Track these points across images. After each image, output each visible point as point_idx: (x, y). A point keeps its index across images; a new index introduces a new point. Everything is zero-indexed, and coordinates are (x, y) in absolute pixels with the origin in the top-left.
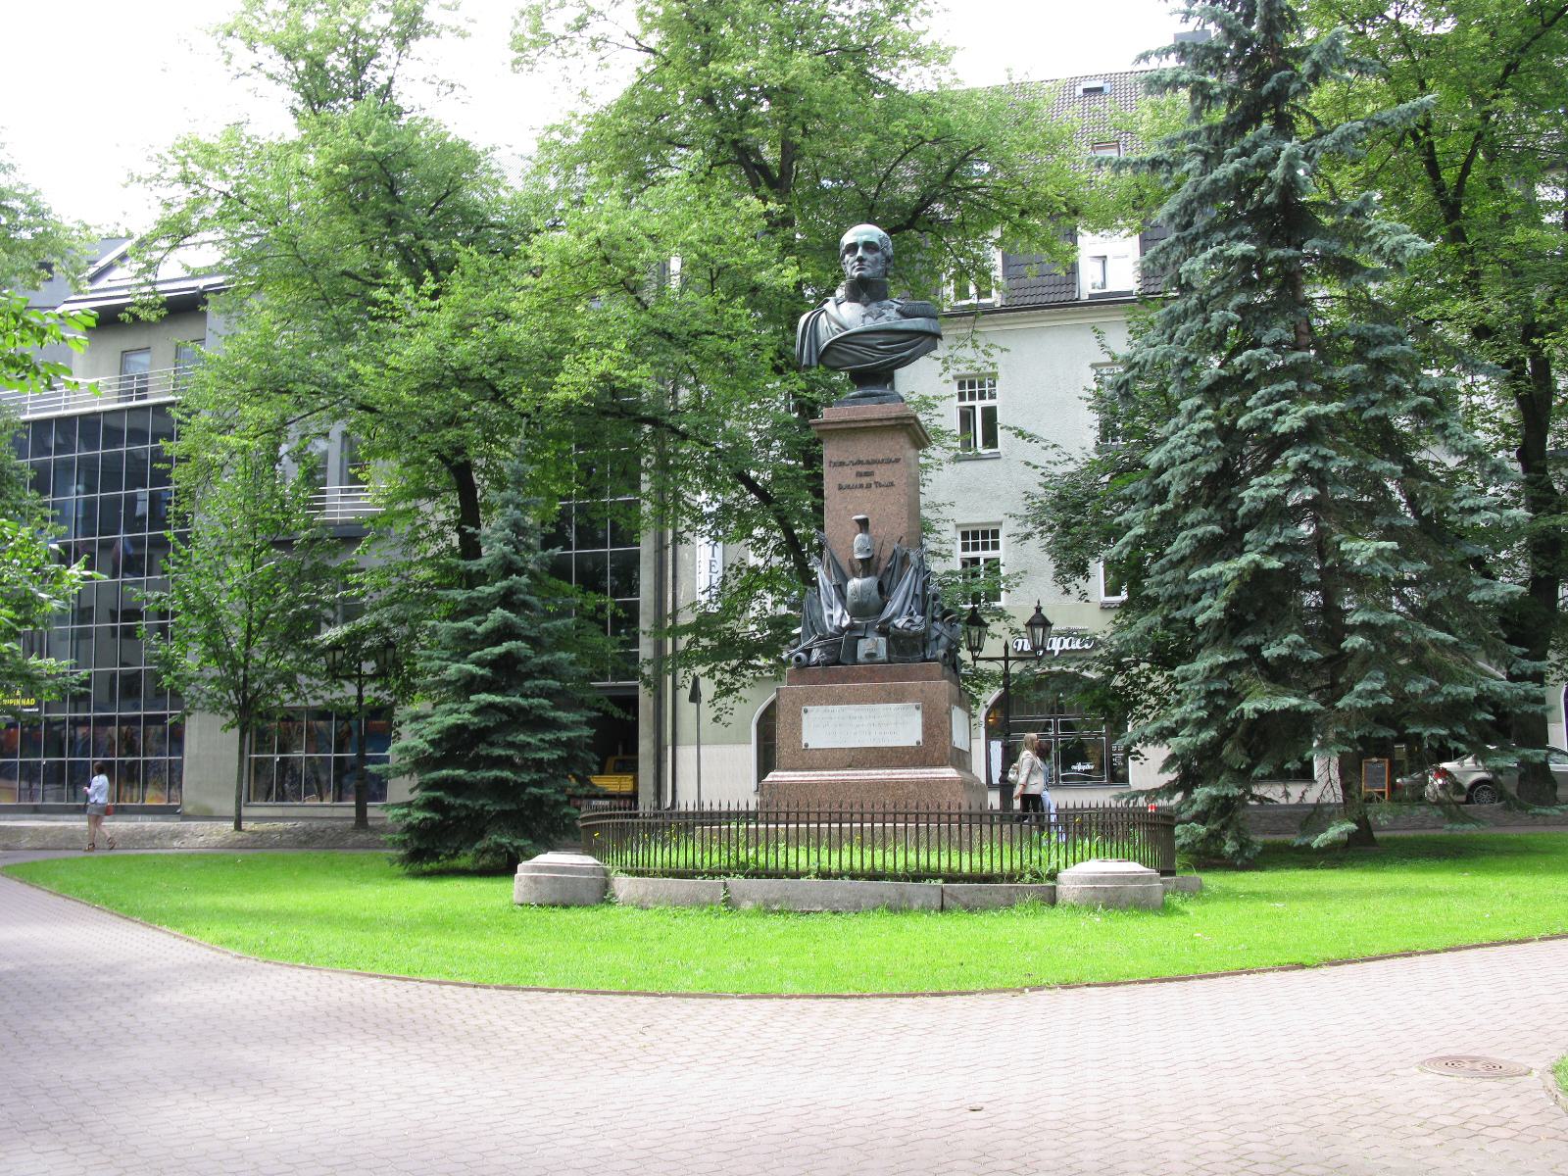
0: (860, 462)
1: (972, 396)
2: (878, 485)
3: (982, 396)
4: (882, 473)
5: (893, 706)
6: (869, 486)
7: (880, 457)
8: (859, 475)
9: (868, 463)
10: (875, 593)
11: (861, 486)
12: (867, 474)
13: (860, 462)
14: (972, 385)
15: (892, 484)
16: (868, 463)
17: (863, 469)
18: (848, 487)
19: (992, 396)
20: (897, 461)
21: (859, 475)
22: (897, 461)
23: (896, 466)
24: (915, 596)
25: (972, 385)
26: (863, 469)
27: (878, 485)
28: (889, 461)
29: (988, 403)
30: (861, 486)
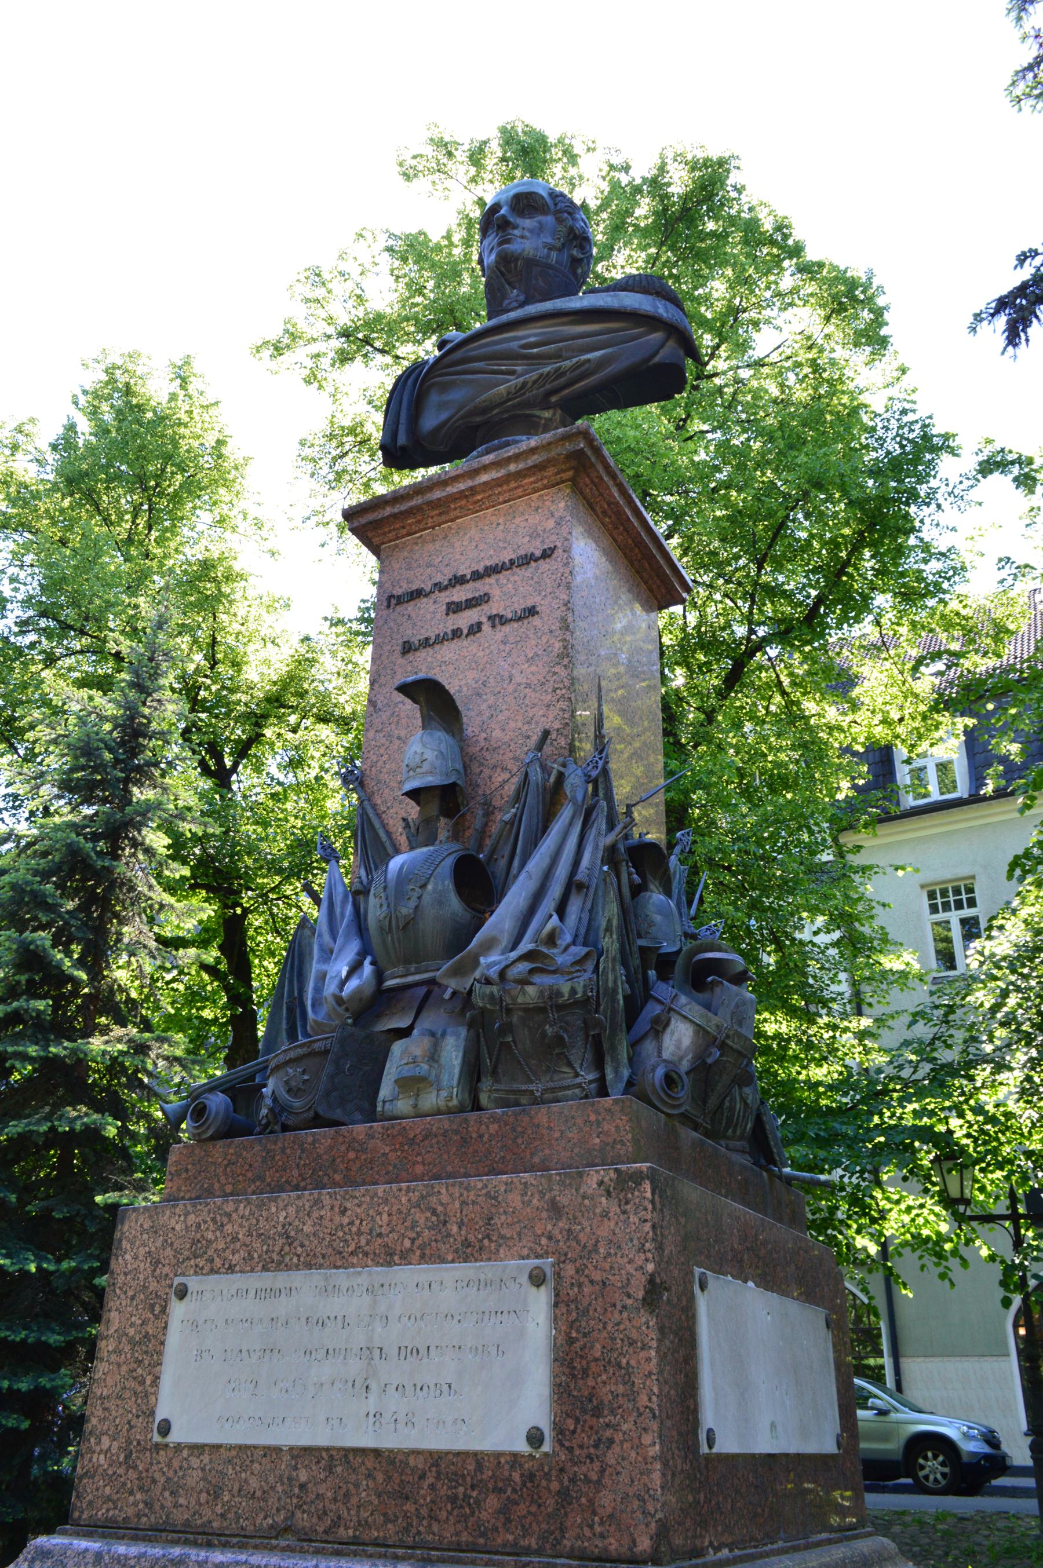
0: (459, 580)
1: (946, 907)
3: (959, 905)
4: (506, 593)
5: (452, 1274)
6: (475, 629)
7: (507, 556)
8: (454, 608)
9: (477, 576)
10: (442, 883)
11: (457, 634)
13: (459, 580)
14: (944, 893)
15: (532, 612)
16: (477, 576)
17: (459, 594)
18: (426, 643)
19: (972, 903)
20: (547, 554)
21: (454, 608)
22: (547, 554)
23: (544, 565)
24: (573, 886)
25: (944, 893)
26: (459, 594)
28: (528, 560)
29: (967, 912)
30: (457, 634)
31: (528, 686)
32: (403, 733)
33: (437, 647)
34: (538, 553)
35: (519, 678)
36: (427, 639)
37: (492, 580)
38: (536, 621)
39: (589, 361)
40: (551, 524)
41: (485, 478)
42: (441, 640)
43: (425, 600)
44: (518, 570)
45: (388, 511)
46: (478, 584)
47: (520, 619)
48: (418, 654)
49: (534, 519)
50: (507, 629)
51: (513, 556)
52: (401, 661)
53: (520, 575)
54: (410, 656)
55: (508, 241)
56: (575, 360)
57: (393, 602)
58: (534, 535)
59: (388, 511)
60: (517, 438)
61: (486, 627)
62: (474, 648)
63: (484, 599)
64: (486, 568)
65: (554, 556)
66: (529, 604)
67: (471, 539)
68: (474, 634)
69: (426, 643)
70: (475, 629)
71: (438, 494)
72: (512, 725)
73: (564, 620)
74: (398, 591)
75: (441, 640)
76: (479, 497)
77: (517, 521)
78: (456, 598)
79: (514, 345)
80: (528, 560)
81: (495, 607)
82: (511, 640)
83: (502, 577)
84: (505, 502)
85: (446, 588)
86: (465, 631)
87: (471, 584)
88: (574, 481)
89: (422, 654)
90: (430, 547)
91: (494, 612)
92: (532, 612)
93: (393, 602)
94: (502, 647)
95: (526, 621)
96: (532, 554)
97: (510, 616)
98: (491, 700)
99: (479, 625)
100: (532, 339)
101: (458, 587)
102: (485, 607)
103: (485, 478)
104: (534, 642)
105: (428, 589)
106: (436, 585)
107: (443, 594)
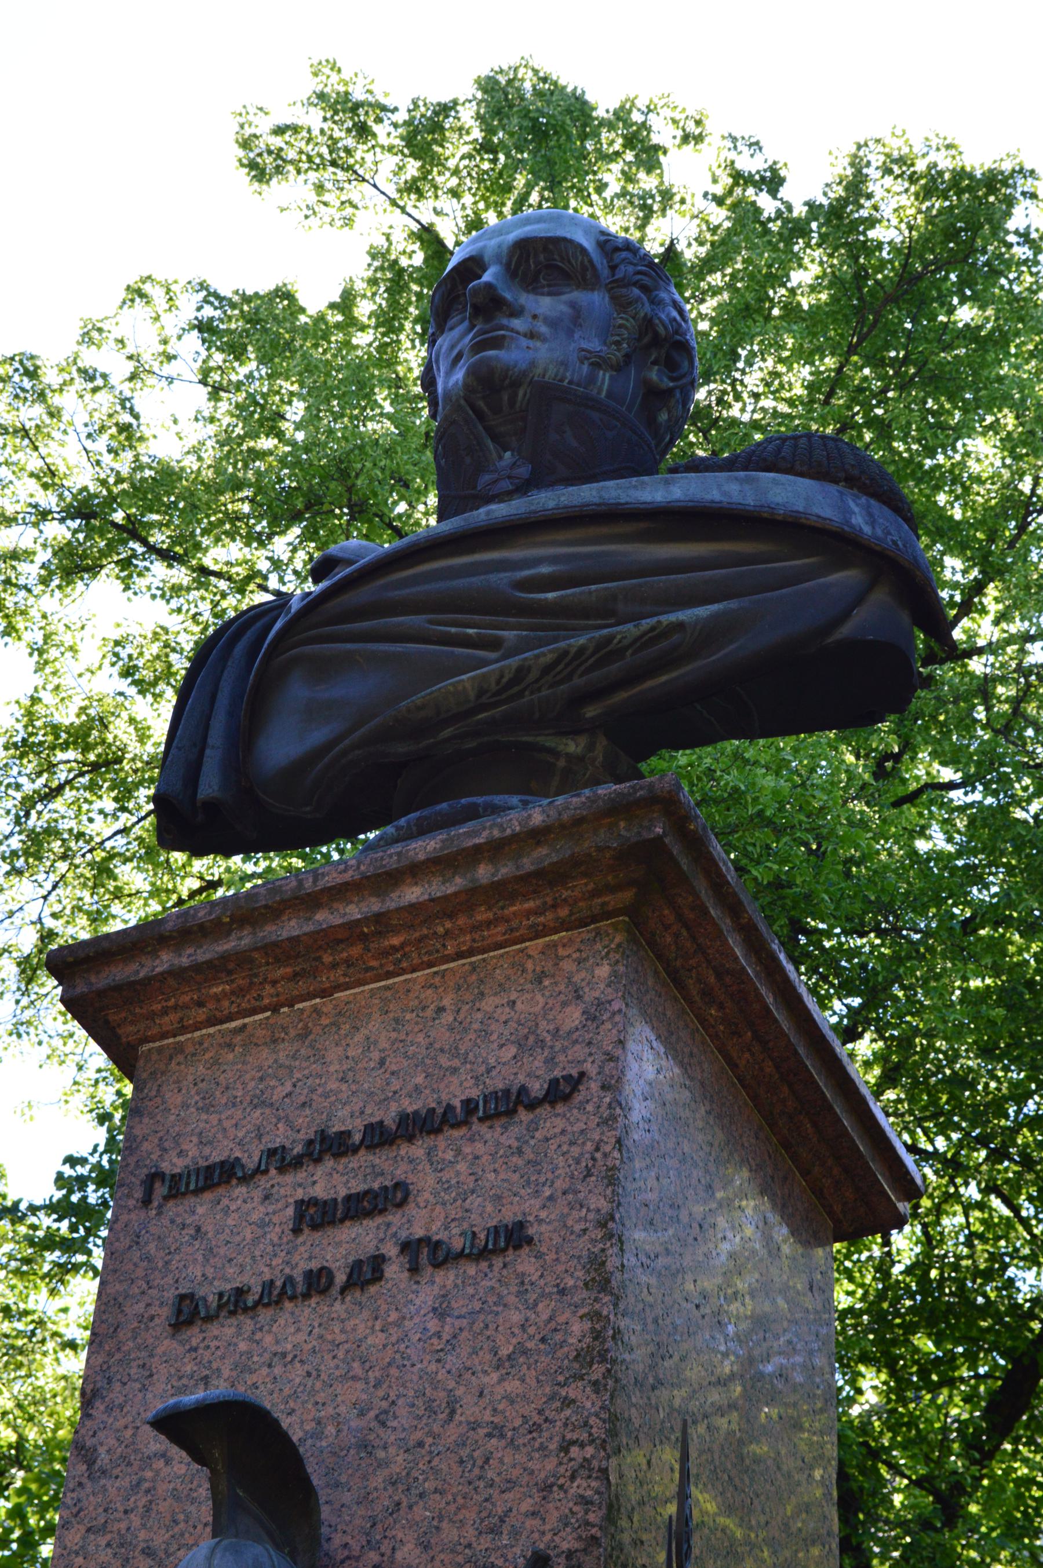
0: (331, 1145)
2: (425, 1254)
4: (451, 1186)
6: (367, 1273)
7: (458, 1090)
8: (314, 1216)
9: (378, 1137)
11: (318, 1282)
12: (360, 1207)
13: (331, 1145)
15: (514, 1237)
16: (378, 1137)
18: (236, 1303)
20: (561, 1092)
21: (314, 1216)
22: (561, 1092)
23: (552, 1122)
27: (425, 1254)
28: (507, 1105)
30: (318, 1282)
31: (497, 1431)
32: (159, 1540)
33: (265, 1315)
34: (537, 1088)
35: (470, 1409)
36: (240, 1292)
37: (417, 1150)
38: (525, 1263)
39: (680, 626)
40: (574, 1016)
41: (413, 894)
42: (277, 1295)
43: (241, 1191)
44: (483, 1129)
45: (166, 960)
46: (380, 1159)
47: (483, 1254)
48: (214, 1329)
49: (531, 1003)
50: (447, 1277)
51: (474, 1093)
52: (167, 1345)
53: (490, 1139)
54: (194, 1335)
55: (497, 343)
56: (646, 623)
57: (160, 1190)
58: (527, 1042)
59: (166, 960)
60: (498, 799)
61: (394, 1271)
62: (360, 1323)
63: (394, 1197)
64: (404, 1118)
65: (578, 1098)
66: (509, 1215)
67: (369, 1044)
68: (364, 1285)
69: (236, 1303)
70: (367, 1273)
71: (291, 927)
72: (450, 1533)
73: (596, 1263)
74: (173, 1164)
75: (277, 1295)
76: (396, 941)
77: (489, 1004)
78: (320, 1191)
79: (501, 579)
80: (507, 1105)
81: (418, 1221)
82: (459, 1305)
83: (443, 1144)
84: (460, 955)
85: (297, 1163)
86: (340, 1278)
87: (364, 1157)
88: (636, 919)
89: (225, 1330)
90: (265, 1056)
91: (419, 1233)
92: (514, 1237)
93: (160, 1190)
94: (433, 1325)
95: (498, 1262)
96: (523, 1090)
97: (457, 1244)
98: (399, 1461)
99: (378, 1262)
100: (545, 570)
101: (329, 1163)
102: (395, 1218)
103: (413, 894)
104: (516, 1317)
105: (251, 1164)
106: (272, 1153)
107: (289, 1178)
